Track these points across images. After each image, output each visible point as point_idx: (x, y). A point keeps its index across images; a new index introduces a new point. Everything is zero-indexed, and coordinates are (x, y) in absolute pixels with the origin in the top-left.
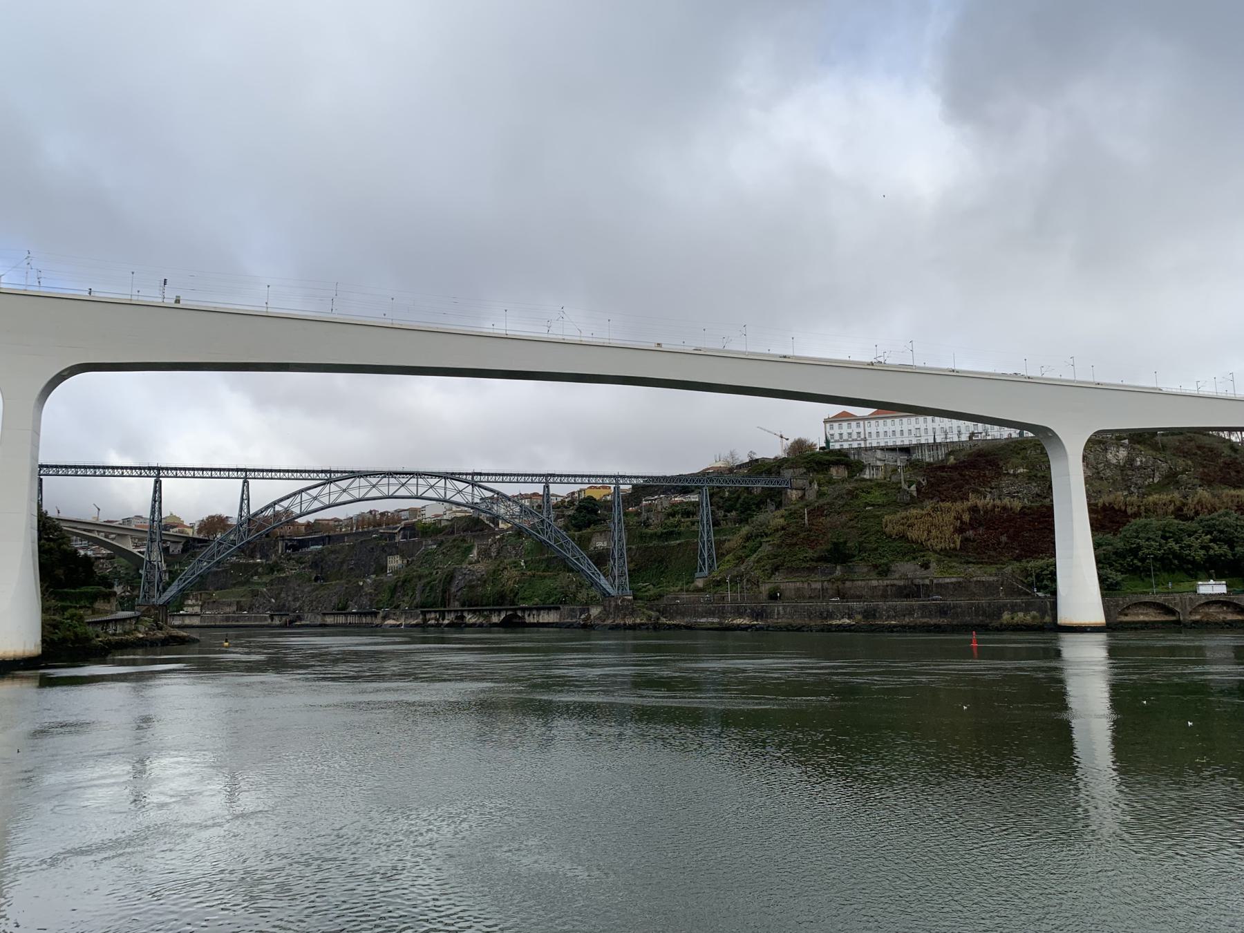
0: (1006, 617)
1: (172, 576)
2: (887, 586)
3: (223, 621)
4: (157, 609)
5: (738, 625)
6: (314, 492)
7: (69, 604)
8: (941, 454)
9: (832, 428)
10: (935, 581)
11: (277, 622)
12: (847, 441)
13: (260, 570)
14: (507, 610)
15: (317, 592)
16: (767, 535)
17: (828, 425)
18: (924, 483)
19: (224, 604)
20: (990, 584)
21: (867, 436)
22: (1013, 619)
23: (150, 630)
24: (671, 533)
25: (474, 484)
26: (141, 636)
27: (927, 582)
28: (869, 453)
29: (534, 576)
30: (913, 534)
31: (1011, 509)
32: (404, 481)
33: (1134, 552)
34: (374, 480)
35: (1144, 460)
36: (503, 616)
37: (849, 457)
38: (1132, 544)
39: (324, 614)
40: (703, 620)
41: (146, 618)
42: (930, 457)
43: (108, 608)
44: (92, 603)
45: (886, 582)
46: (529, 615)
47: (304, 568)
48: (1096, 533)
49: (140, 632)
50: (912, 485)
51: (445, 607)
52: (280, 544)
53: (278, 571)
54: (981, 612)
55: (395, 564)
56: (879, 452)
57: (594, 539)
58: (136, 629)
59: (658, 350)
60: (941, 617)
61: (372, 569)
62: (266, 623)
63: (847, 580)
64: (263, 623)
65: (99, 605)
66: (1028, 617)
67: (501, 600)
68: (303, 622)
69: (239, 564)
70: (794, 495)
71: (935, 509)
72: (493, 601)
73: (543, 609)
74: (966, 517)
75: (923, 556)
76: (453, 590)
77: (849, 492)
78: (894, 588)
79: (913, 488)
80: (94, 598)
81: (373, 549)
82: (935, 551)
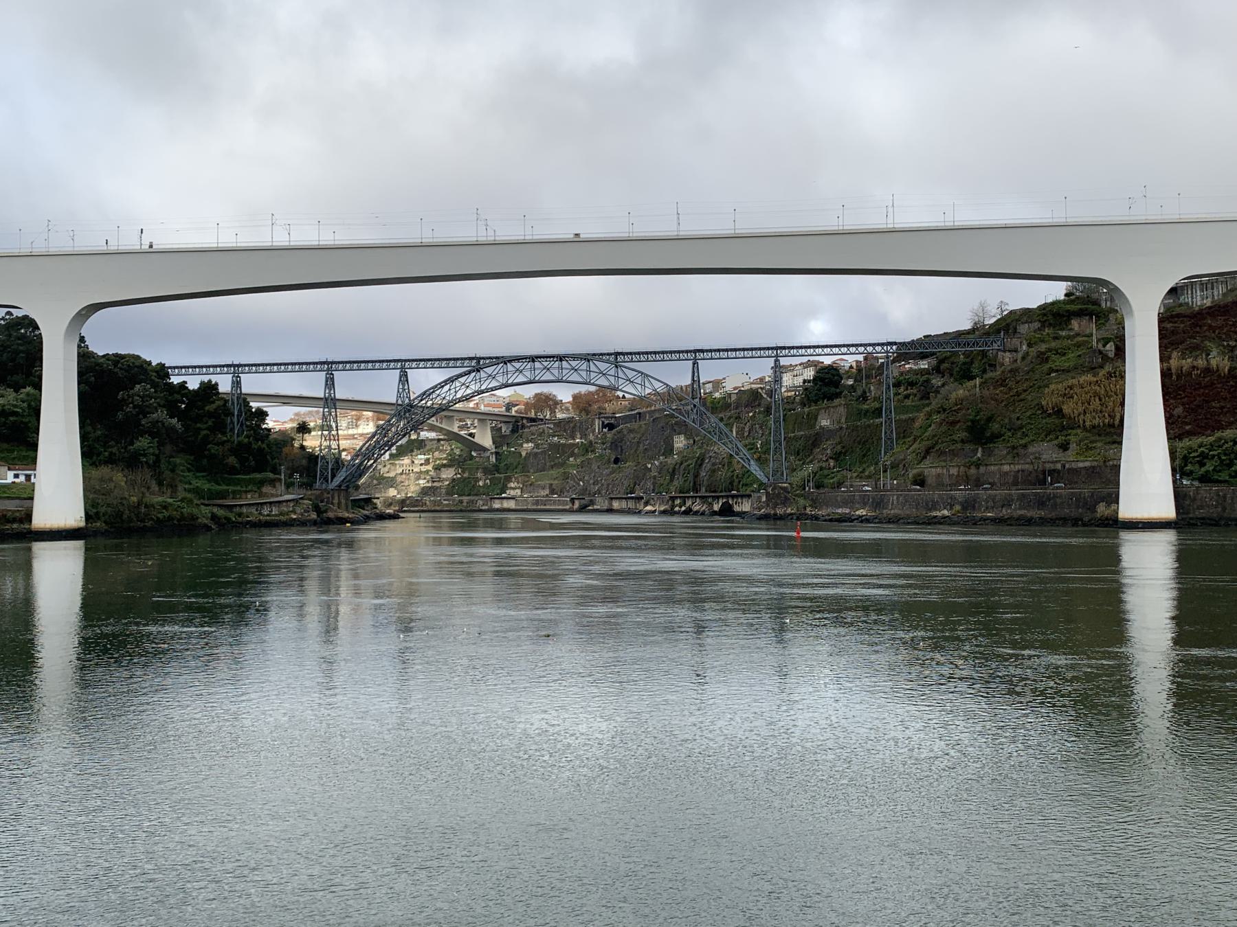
1: (498, 457)
2: (1018, 471)
4: (328, 493)
7: (239, 488)
8: (1219, 291)
10: (1067, 466)
13: (232, 460)
14: (722, 497)
15: (613, 475)
23: (305, 511)
26: (295, 517)
27: (1059, 466)
31: (1218, 370)
34: (517, 365)
37: (1100, 305)
39: (612, 499)
40: (840, 511)
45: (1018, 467)
49: (295, 513)
50: (1108, 343)
55: (681, 445)
57: (819, 417)
58: (294, 512)
59: (577, 240)
60: (1038, 509)
62: (568, 507)
65: (266, 489)
68: (595, 507)
80: (262, 483)
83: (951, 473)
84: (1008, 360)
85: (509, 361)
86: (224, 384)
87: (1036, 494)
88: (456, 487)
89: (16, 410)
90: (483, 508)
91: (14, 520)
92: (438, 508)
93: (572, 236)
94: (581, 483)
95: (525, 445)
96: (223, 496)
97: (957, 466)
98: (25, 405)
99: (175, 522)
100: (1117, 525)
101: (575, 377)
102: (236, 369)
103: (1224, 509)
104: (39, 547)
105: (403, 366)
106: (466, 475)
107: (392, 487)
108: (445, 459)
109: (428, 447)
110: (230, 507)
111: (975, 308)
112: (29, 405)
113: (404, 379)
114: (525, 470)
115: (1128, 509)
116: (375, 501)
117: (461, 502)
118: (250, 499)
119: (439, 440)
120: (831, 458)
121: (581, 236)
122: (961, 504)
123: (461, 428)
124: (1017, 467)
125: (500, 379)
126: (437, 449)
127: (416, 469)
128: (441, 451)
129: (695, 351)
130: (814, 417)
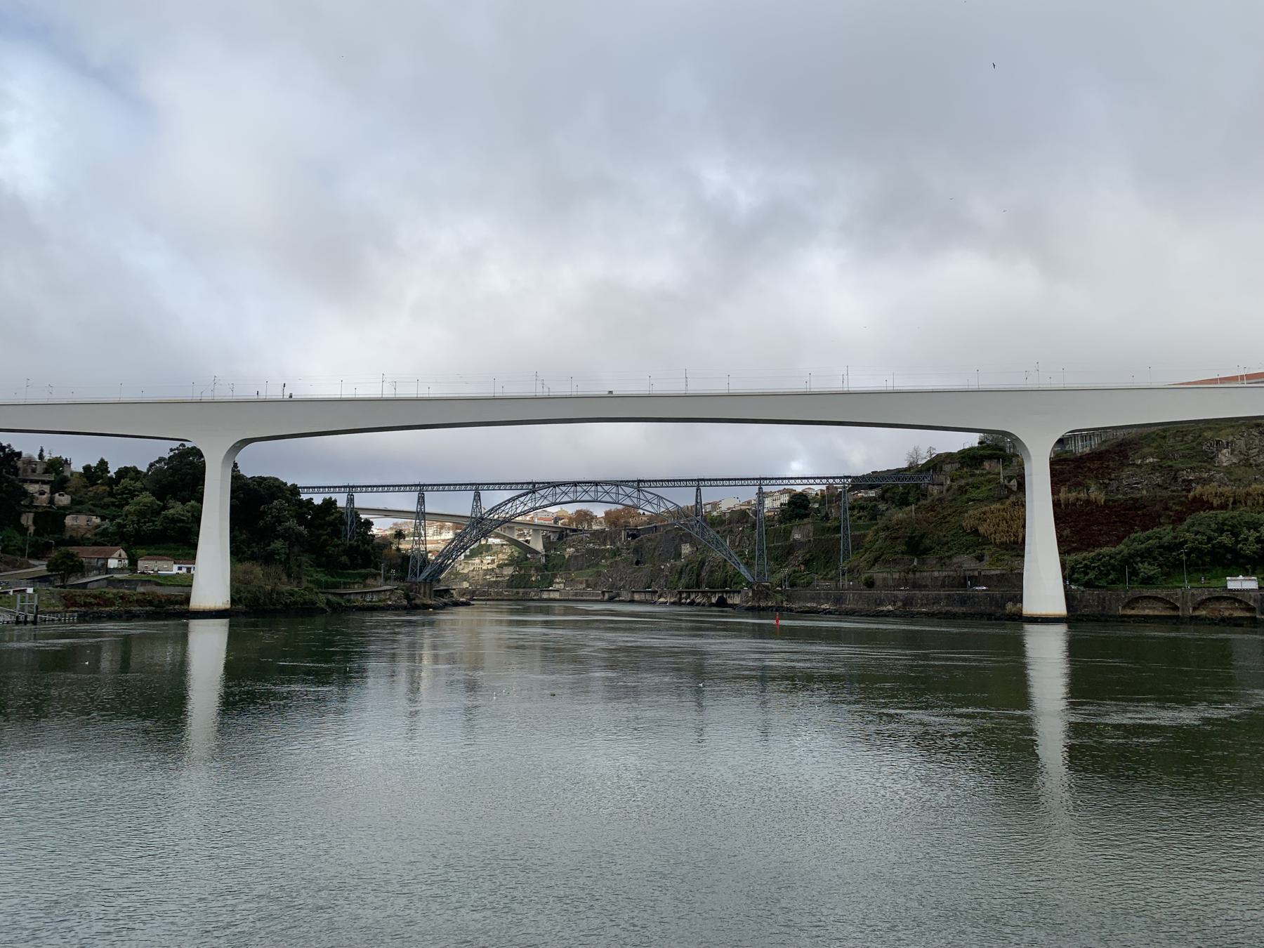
2: (945, 577)
4: (417, 585)
5: (824, 610)
7: (349, 580)
8: (1095, 442)
10: (983, 573)
13: (344, 559)
14: (719, 592)
19: (577, 582)
27: (976, 573)
31: (1096, 502)
34: (563, 488)
37: (1005, 451)
43: (375, 583)
45: (945, 574)
47: (629, 554)
49: (391, 600)
51: (699, 589)
54: (994, 603)
55: (687, 551)
57: (793, 532)
58: (390, 599)
59: (611, 395)
61: (673, 556)
62: (599, 598)
65: (370, 581)
68: (621, 598)
80: (365, 577)
81: (673, 538)
83: (894, 576)
84: (936, 491)
85: (557, 485)
86: (341, 501)
87: (959, 595)
88: (513, 582)
89: (183, 518)
90: (535, 598)
91: (177, 603)
92: (500, 598)
93: (607, 393)
94: (610, 580)
95: (568, 550)
96: (336, 586)
97: (899, 572)
98: (190, 514)
100: (1021, 619)
101: (607, 498)
102: (351, 489)
103: (1104, 608)
104: (195, 624)
105: (477, 488)
106: (522, 572)
107: (465, 581)
108: (507, 559)
109: (494, 550)
110: (342, 595)
111: (911, 452)
112: (193, 515)
113: (477, 498)
114: (567, 569)
115: (1031, 606)
116: (452, 591)
117: (518, 593)
118: (357, 588)
119: (502, 545)
120: (802, 564)
121: (614, 393)
122: (901, 601)
123: (520, 536)
124: (944, 573)
125: (550, 499)
126: (501, 552)
127: (484, 568)
128: (504, 553)
129: (699, 480)
130: (788, 533)
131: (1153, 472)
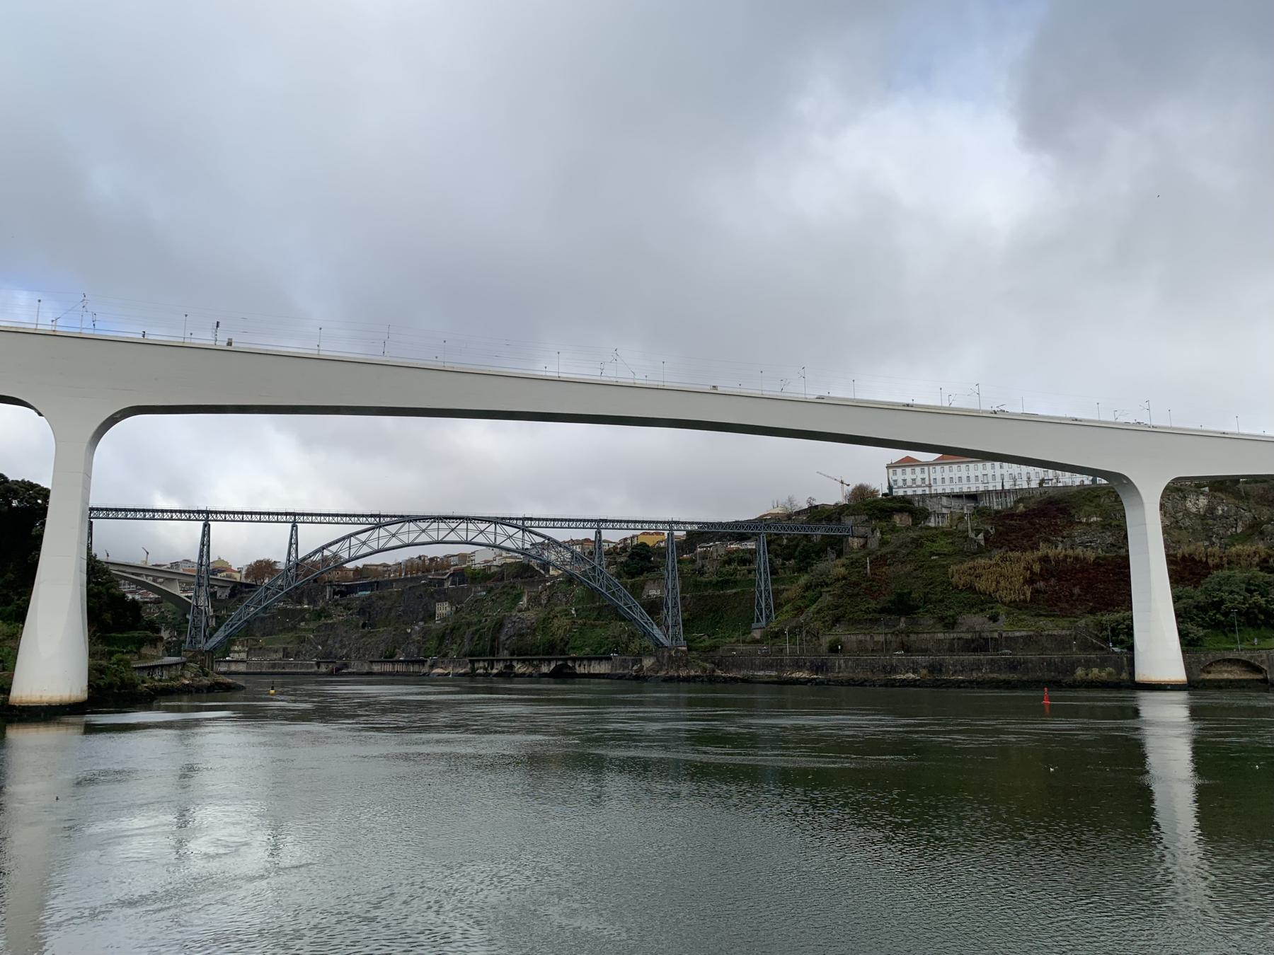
0: (1080, 672)
2: (954, 639)
3: (269, 668)
4: (203, 655)
5: (797, 679)
6: (363, 537)
8: (1010, 501)
9: (895, 473)
10: (1004, 635)
11: (323, 669)
12: (911, 487)
14: (557, 660)
16: (827, 585)
17: (891, 470)
18: (992, 532)
19: (270, 650)
20: (1063, 637)
21: (932, 482)
22: (1087, 675)
24: (727, 582)
25: (524, 529)
26: (187, 682)
27: (996, 635)
28: (935, 499)
29: (585, 624)
30: (981, 585)
32: (453, 525)
33: (1217, 605)
34: (423, 525)
35: (1226, 509)
36: (553, 666)
38: (1215, 597)
39: (371, 662)
40: (761, 673)
41: (192, 664)
42: (998, 505)
44: (139, 649)
46: (580, 666)
47: (351, 614)
48: (1175, 585)
49: (186, 678)
51: (494, 656)
52: (328, 589)
53: (325, 617)
55: (444, 611)
56: (944, 499)
57: (646, 587)
58: (182, 676)
59: (714, 393)
60: (1011, 673)
61: (421, 616)
62: (313, 670)
63: (911, 633)
64: (310, 671)
65: (145, 650)
66: (1103, 674)
67: (551, 649)
68: (350, 670)
69: (285, 609)
70: (855, 543)
71: (1004, 559)
72: (543, 651)
73: (596, 659)
74: (1037, 568)
75: (992, 608)
76: (503, 638)
77: (914, 541)
78: (960, 642)
79: (981, 536)
80: (140, 643)
82: (1004, 604)
83: (876, 639)
99: (116, 691)
124: (952, 635)
131: (1104, 530)
